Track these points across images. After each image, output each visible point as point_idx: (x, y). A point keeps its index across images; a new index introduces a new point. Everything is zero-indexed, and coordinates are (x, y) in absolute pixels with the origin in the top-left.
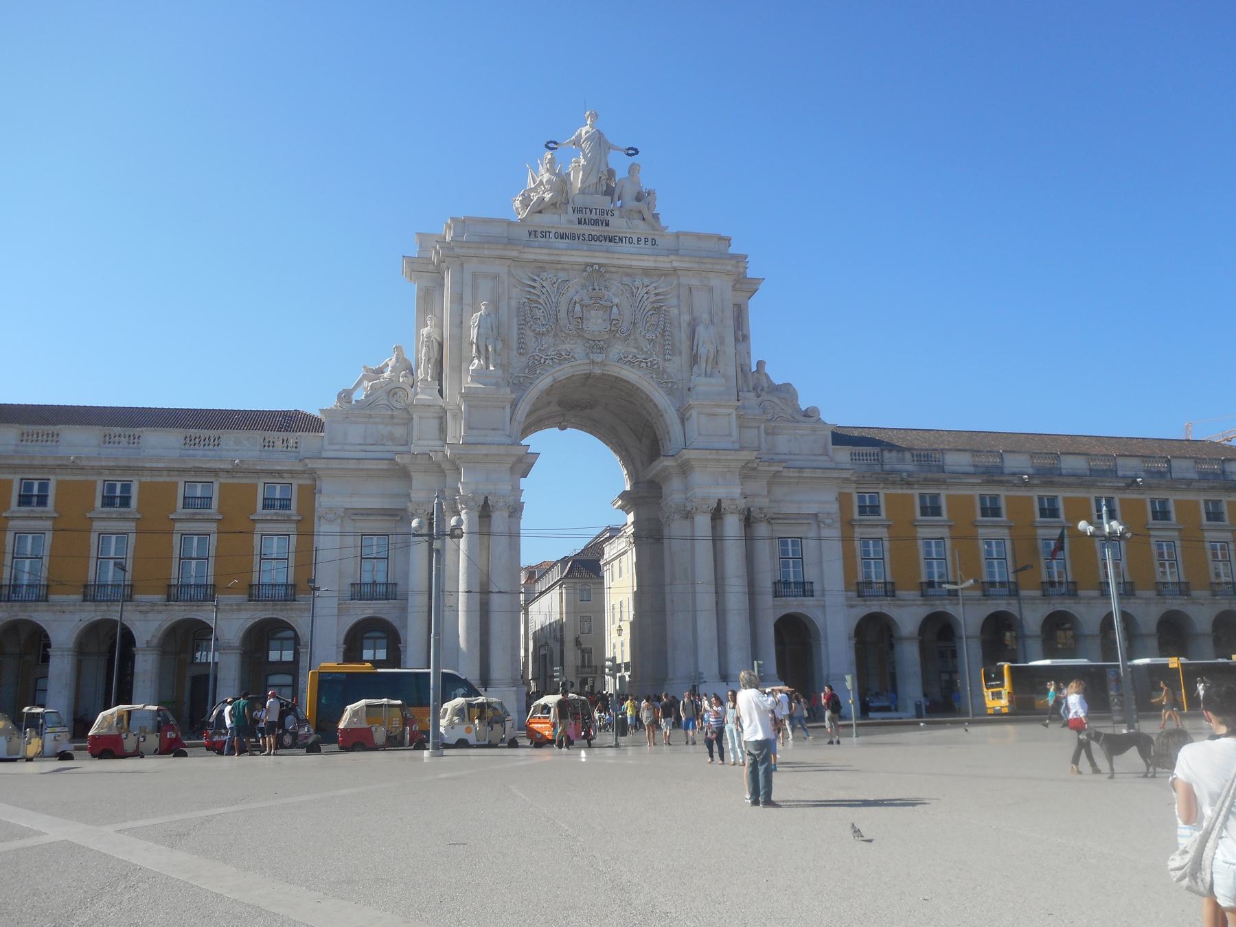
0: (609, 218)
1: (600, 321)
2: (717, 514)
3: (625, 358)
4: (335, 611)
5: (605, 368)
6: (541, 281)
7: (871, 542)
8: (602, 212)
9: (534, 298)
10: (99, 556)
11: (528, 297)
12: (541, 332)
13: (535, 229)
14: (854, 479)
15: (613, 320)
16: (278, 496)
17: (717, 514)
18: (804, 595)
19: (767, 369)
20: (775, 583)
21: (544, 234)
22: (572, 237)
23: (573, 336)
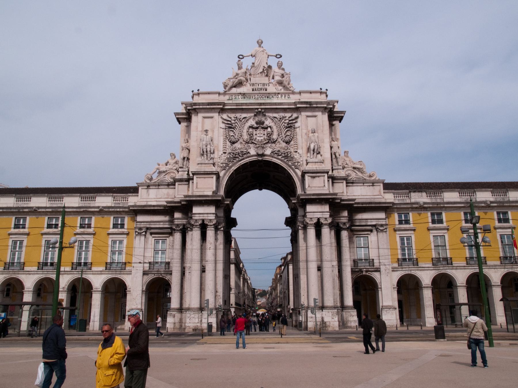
0: (267, 87)
2: (318, 226)
4: (142, 274)
7: (405, 238)
8: (264, 85)
9: (230, 126)
10: (45, 250)
11: (228, 126)
15: (268, 134)
16: (119, 223)
17: (318, 226)
19: (349, 155)
23: (248, 143)
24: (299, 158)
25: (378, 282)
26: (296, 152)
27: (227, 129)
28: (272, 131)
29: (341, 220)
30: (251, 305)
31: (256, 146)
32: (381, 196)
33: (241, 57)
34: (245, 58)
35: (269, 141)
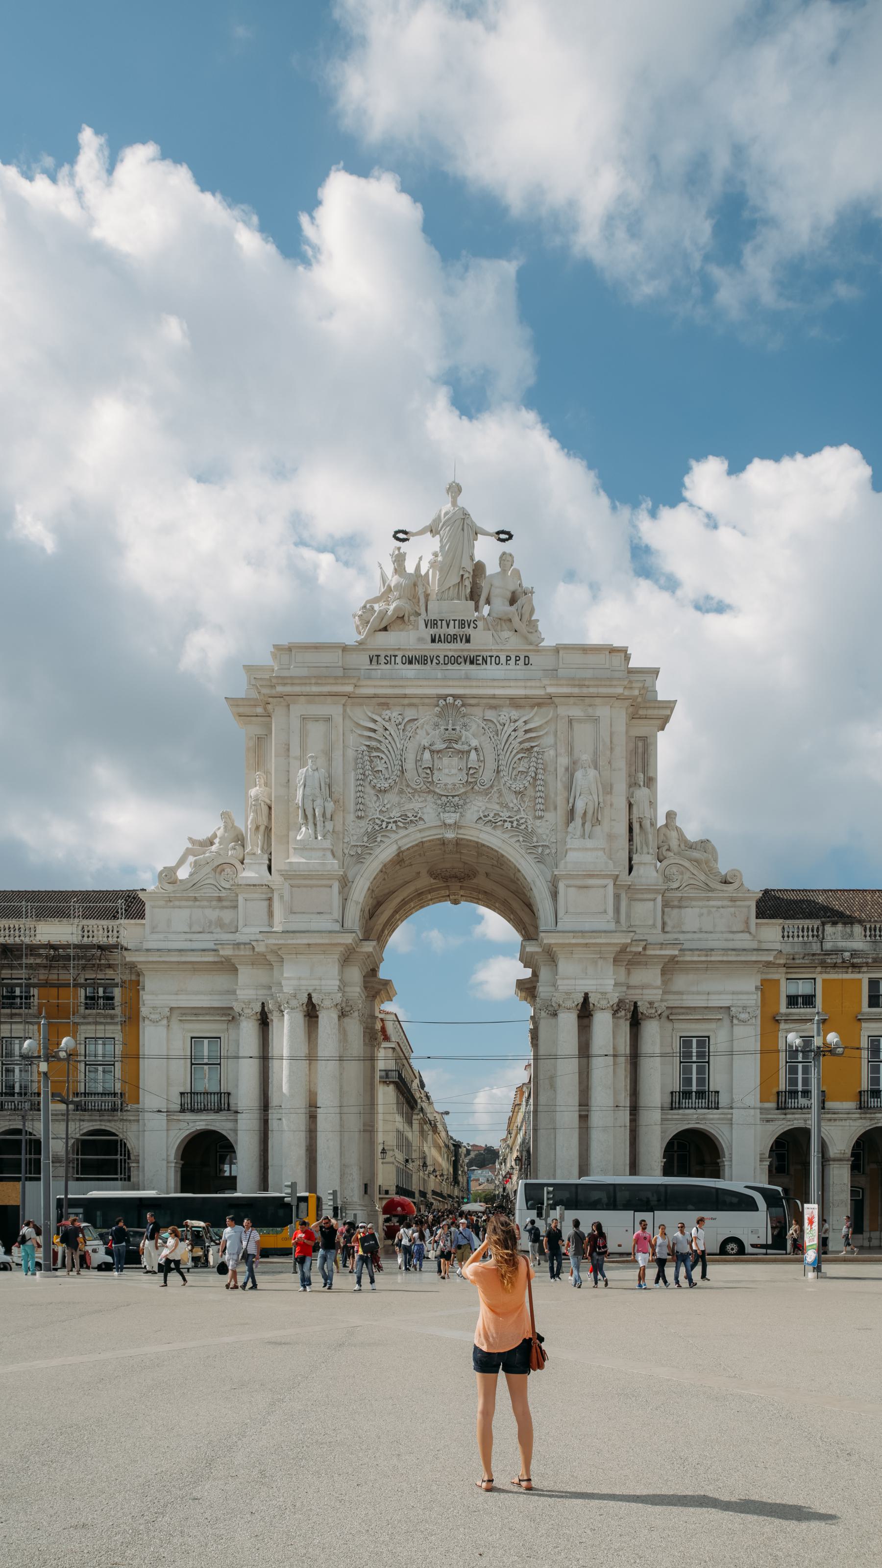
1: (454, 771)
3: (485, 816)
5: (460, 831)
6: (384, 723)
8: (462, 624)
9: (374, 744)
11: (368, 743)
12: (383, 788)
13: (378, 653)
14: (782, 961)
15: (470, 768)
18: (708, 1108)
20: (672, 1093)
21: (388, 659)
22: (423, 660)
23: (421, 792)
24: (547, 836)
25: (724, 1146)
26: (541, 817)
27: (364, 753)
28: (481, 761)
29: (644, 997)
30: (445, 1193)
31: (439, 802)
32: (750, 933)
33: (402, 536)
34: (412, 538)
35: (473, 788)
